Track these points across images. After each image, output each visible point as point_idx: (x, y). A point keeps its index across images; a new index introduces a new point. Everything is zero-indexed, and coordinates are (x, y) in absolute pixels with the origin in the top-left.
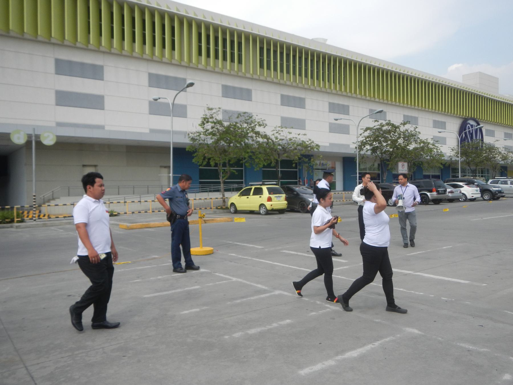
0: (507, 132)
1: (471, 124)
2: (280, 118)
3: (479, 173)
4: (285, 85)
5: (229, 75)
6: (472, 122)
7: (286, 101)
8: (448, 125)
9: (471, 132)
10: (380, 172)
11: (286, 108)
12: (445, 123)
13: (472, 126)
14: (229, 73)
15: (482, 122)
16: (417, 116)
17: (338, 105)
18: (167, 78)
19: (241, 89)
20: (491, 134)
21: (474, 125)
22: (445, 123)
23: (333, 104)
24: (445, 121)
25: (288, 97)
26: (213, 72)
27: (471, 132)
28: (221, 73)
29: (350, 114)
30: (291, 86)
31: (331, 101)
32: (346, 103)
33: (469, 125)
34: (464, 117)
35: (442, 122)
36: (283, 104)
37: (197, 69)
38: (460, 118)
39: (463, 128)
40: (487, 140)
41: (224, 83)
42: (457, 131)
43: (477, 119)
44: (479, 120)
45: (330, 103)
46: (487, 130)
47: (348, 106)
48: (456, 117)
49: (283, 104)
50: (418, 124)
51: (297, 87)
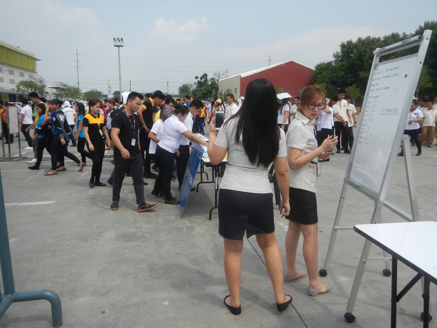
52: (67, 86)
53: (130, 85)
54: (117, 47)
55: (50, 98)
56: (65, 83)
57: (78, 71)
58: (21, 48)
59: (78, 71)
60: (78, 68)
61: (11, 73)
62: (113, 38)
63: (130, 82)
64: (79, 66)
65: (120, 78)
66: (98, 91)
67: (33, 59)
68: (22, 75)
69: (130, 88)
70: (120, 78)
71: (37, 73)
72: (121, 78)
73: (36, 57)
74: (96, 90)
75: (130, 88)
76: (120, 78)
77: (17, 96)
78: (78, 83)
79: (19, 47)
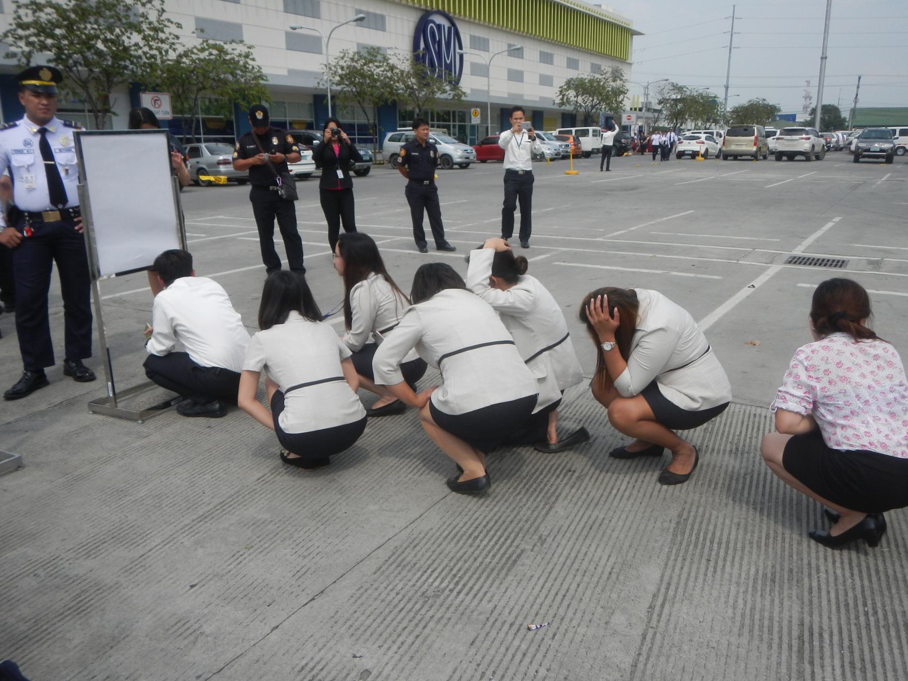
1: (438, 22)
3: (454, 121)
6: (439, 20)
8: (390, 23)
12: (383, 17)
13: (439, 27)
15: (463, 21)
20: (480, 44)
22: (383, 17)
24: (384, 13)
33: (431, 24)
34: (423, 7)
38: (416, 9)
39: (421, 29)
40: (471, 56)
43: (451, 15)
44: (457, 16)
46: (473, 39)
52: (685, 89)
53: (858, 87)
55: (629, 119)
56: (680, 84)
57: (730, 57)
58: (602, 7)
59: (730, 57)
60: (730, 50)
61: (572, 64)
63: (860, 78)
64: (733, 46)
65: (822, 58)
66: (768, 105)
67: (625, 32)
68: (596, 68)
69: (857, 95)
70: (824, 58)
71: (631, 64)
72: (826, 58)
73: (634, 27)
74: (764, 100)
75: (857, 95)
76: (824, 58)
77: (580, 118)
78: (727, 87)
79: (600, 6)
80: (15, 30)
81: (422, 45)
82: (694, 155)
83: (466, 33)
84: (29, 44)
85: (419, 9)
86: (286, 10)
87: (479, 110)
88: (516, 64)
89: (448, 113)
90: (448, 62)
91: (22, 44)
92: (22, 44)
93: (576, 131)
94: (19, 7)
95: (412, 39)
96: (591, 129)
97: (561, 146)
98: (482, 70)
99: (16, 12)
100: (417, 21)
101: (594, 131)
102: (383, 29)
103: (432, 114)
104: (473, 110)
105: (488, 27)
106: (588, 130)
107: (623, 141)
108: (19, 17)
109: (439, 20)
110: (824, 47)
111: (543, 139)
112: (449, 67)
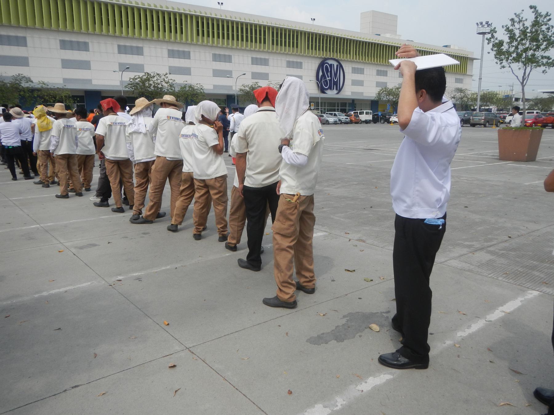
0: (380, 69)
2: (118, 64)
4: (120, 37)
5: (65, 32)
6: (330, 62)
7: (122, 50)
9: (329, 71)
10: (226, 106)
11: (123, 56)
12: (301, 63)
14: (65, 30)
15: (348, 61)
16: (267, 58)
17: (178, 51)
18: (9, 37)
19: (78, 43)
20: (361, 71)
21: (334, 65)
23: (173, 50)
24: (302, 61)
25: (125, 46)
26: (50, 30)
27: (329, 71)
28: (58, 31)
29: (191, 58)
30: (127, 38)
31: (170, 48)
32: (186, 50)
34: (323, 57)
35: (297, 62)
36: (120, 52)
37: (34, 28)
41: (61, 38)
42: (315, 70)
43: (340, 59)
45: (169, 50)
47: (189, 52)
48: (314, 57)
49: (120, 52)
50: (268, 64)
51: (133, 38)
54: (482, 35)
58: (451, 47)
62: (476, 24)
70: (480, 79)
71: (472, 75)
72: (481, 79)
80: (128, 86)
81: (321, 74)
82: (395, 122)
83: (348, 68)
84: (132, 89)
85: (321, 58)
86: (252, 64)
87: (313, 103)
88: (382, 79)
89: (335, 104)
90: (335, 80)
91: (131, 88)
92: (131, 88)
93: (360, 112)
94: (130, 79)
95: (316, 71)
96: (365, 111)
97: (343, 118)
98: (355, 83)
99: (129, 81)
100: (320, 63)
101: (366, 112)
102: (301, 68)
103: (338, 104)
104: (311, 103)
105: (363, 63)
106: (363, 112)
107: (387, 117)
108: (131, 82)
109: (330, 62)
110: (481, 74)
111: (337, 116)
112: (336, 83)
